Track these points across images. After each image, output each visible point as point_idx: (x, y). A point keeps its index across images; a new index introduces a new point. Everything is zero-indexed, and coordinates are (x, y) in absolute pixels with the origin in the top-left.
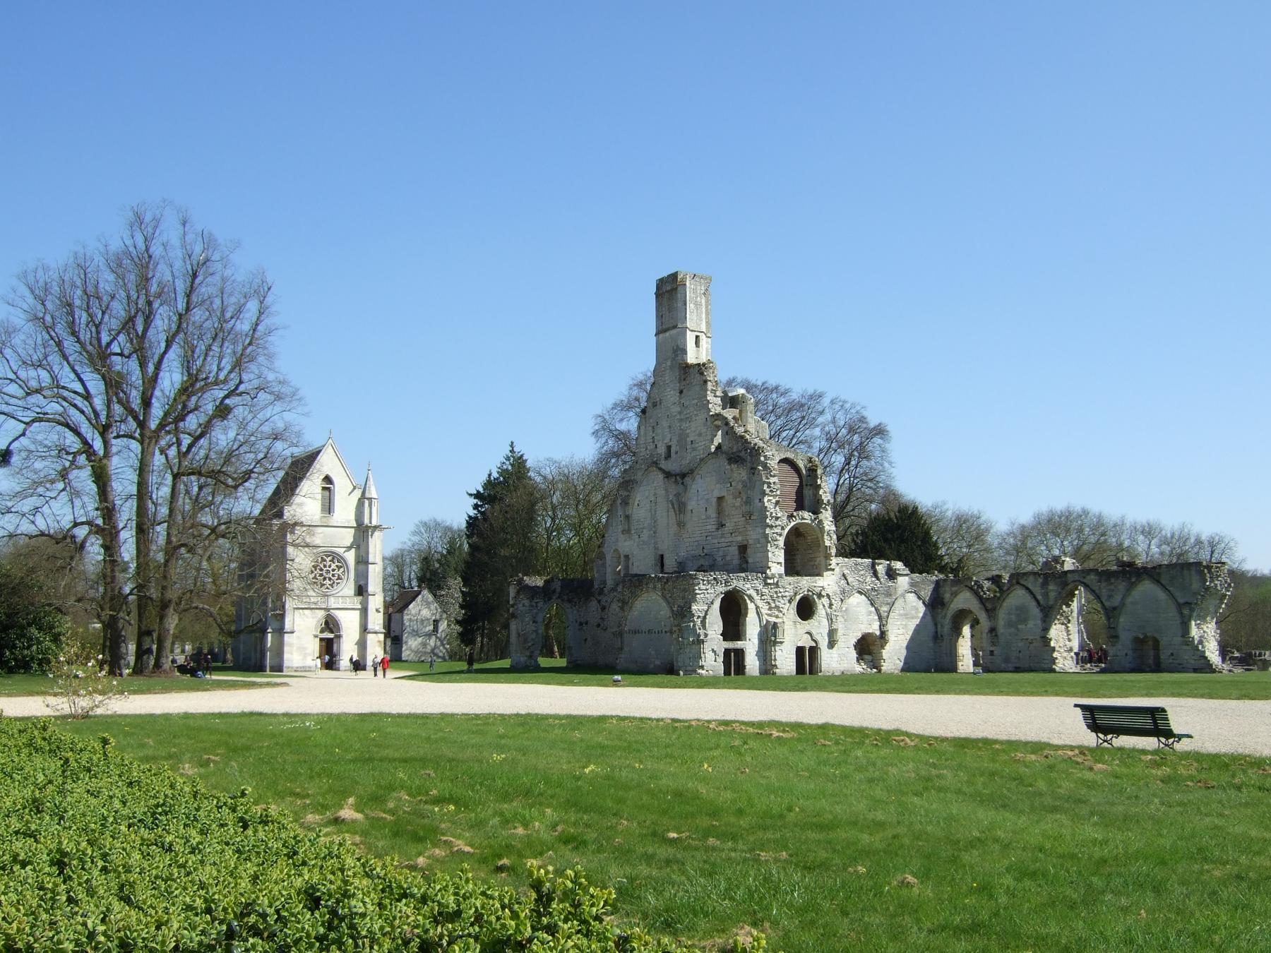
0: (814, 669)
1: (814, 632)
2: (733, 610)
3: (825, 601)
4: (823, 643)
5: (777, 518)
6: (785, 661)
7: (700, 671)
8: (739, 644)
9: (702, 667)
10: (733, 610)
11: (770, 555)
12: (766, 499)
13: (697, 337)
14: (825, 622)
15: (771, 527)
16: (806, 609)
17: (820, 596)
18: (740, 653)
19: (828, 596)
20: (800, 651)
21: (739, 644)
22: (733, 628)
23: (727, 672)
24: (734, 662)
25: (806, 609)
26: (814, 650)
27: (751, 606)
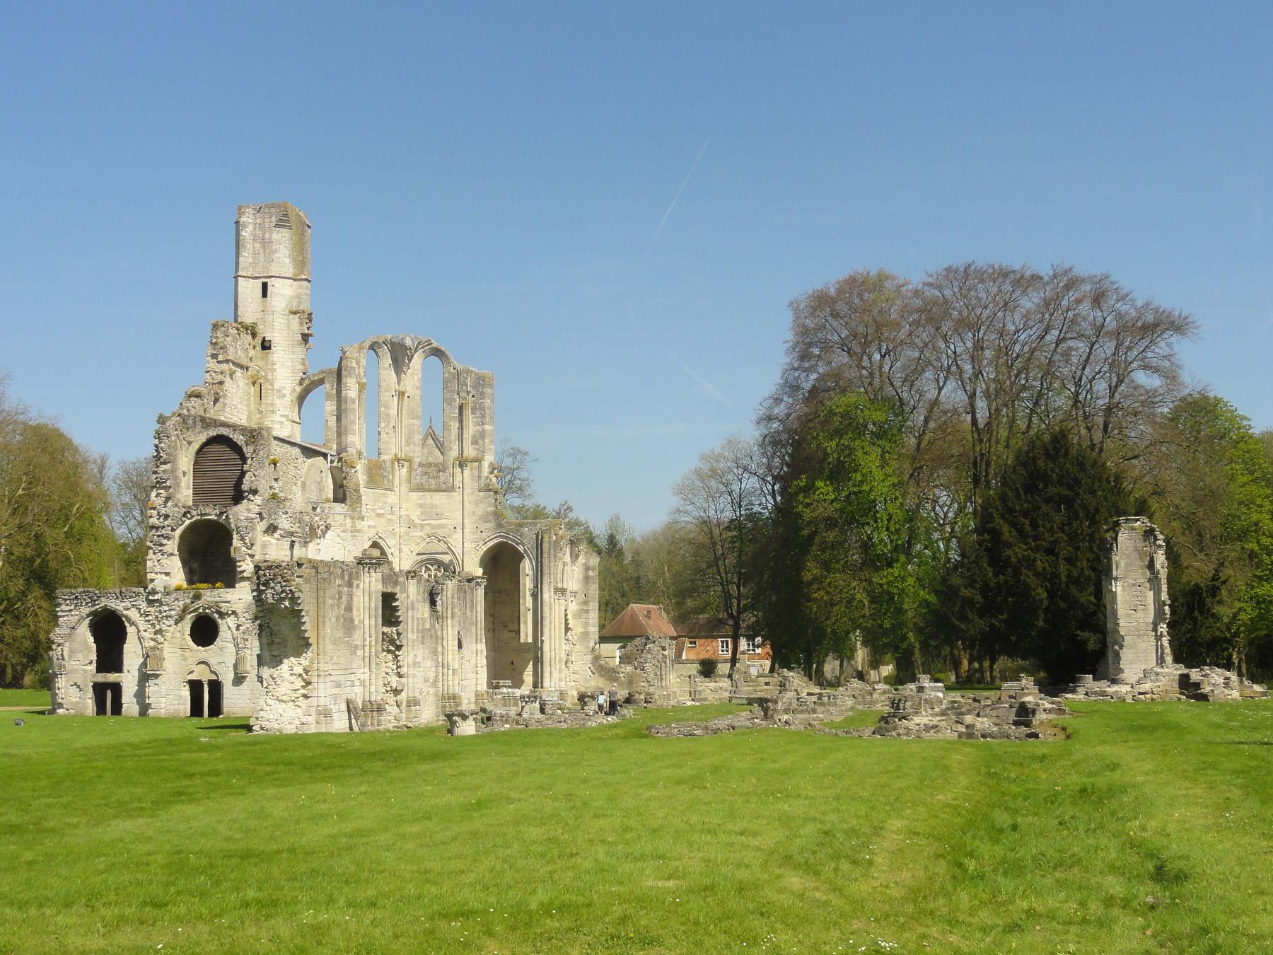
0: (216, 709)
1: (212, 661)
2: (110, 632)
3: (231, 621)
4: (227, 678)
5: (167, 517)
6: (170, 698)
7: (60, 711)
8: (112, 677)
9: (60, 706)
10: (110, 632)
11: (149, 563)
12: (154, 493)
13: (265, 286)
14: (230, 648)
15: (157, 528)
16: (205, 631)
17: (222, 615)
18: (116, 689)
19: (234, 612)
20: (195, 687)
21: (112, 677)
22: (110, 658)
23: (101, 709)
24: (107, 697)
25: (205, 631)
26: (216, 687)
27: (131, 630)
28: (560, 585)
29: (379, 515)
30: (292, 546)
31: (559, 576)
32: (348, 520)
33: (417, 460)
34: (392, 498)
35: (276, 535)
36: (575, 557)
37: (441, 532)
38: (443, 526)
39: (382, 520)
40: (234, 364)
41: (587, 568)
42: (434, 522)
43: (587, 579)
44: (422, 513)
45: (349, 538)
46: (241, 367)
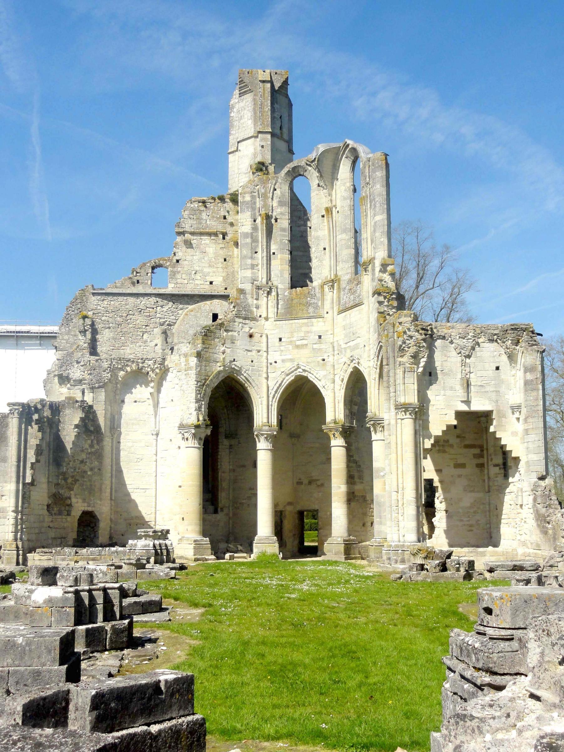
28: (402, 400)
29: (298, 347)
30: (83, 393)
31: (400, 388)
32: (183, 359)
33: (348, 277)
34: (318, 326)
35: (69, 385)
36: (511, 357)
37: (356, 353)
38: (356, 347)
39: (305, 352)
40: (192, 234)
41: (527, 370)
42: (352, 344)
43: (526, 383)
44: (346, 336)
45: (183, 377)
46: (209, 234)
